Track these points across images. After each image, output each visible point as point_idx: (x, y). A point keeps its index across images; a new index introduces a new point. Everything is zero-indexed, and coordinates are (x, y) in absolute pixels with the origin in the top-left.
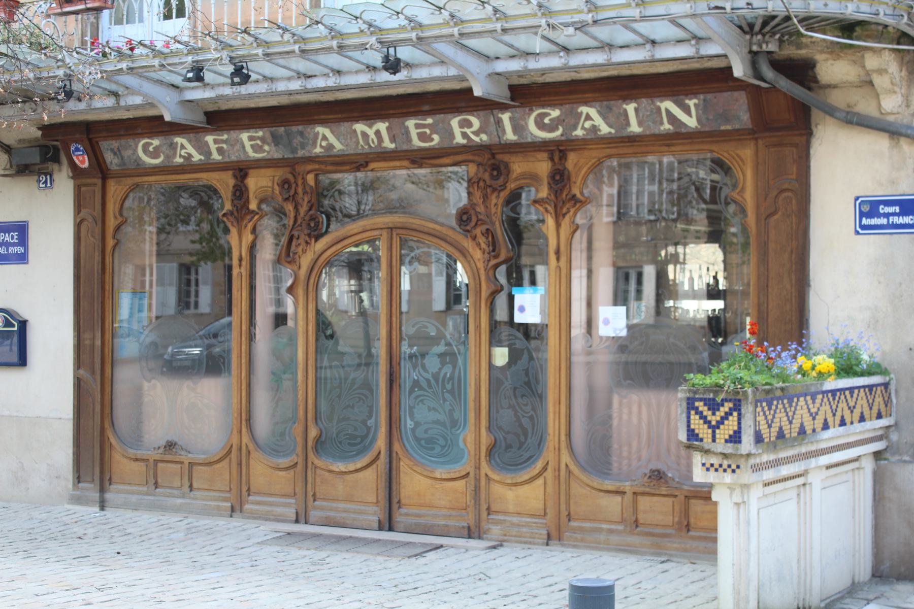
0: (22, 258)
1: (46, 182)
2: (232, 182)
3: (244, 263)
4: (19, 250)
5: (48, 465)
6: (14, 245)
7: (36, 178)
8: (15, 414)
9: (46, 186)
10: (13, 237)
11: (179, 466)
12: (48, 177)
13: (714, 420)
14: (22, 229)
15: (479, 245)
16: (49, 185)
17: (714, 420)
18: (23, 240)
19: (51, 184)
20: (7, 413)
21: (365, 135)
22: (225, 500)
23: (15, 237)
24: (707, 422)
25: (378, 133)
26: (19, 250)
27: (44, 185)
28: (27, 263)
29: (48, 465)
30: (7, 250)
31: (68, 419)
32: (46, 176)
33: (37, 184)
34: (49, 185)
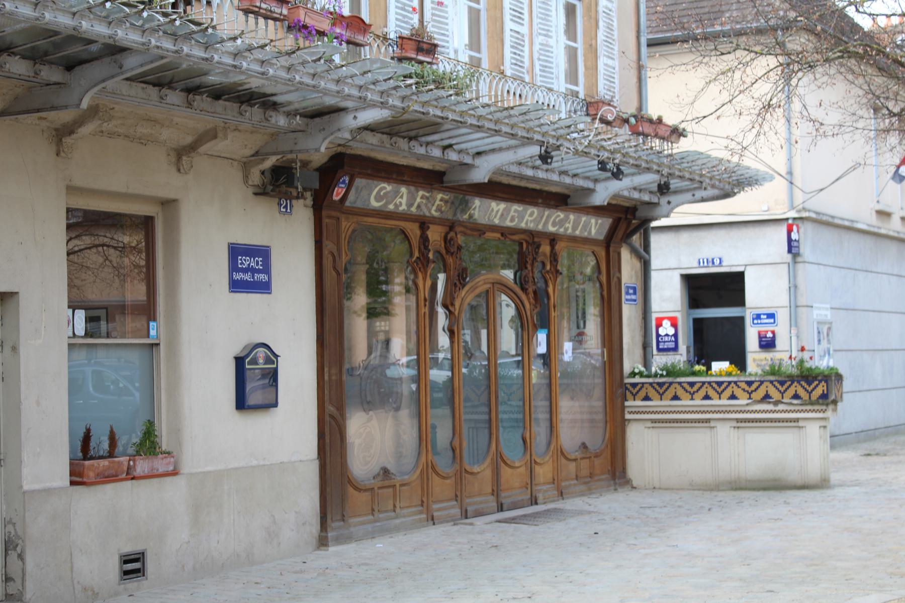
0: (265, 287)
1: (286, 207)
2: (418, 232)
3: (427, 303)
4: (262, 277)
5: (296, 512)
6: (259, 271)
7: (277, 200)
8: (262, 463)
9: (286, 211)
10: (257, 264)
11: (391, 490)
12: (288, 201)
13: (810, 389)
14: (263, 253)
15: (528, 299)
16: (289, 210)
17: (810, 389)
18: (267, 270)
19: (290, 209)
20: (255, 463)
21: (493, 210)
22: (421, 512)
23: (260, 263)
24: (806, 390)
25: (498, 211)
26: (262, 277)
27: (284, 210)
28: (270, 293)
29: (296, 512)
30: (253, 278)
31: (312, 460)
32: (286, 200)
33: (277, 206)
34: (289, 210)
